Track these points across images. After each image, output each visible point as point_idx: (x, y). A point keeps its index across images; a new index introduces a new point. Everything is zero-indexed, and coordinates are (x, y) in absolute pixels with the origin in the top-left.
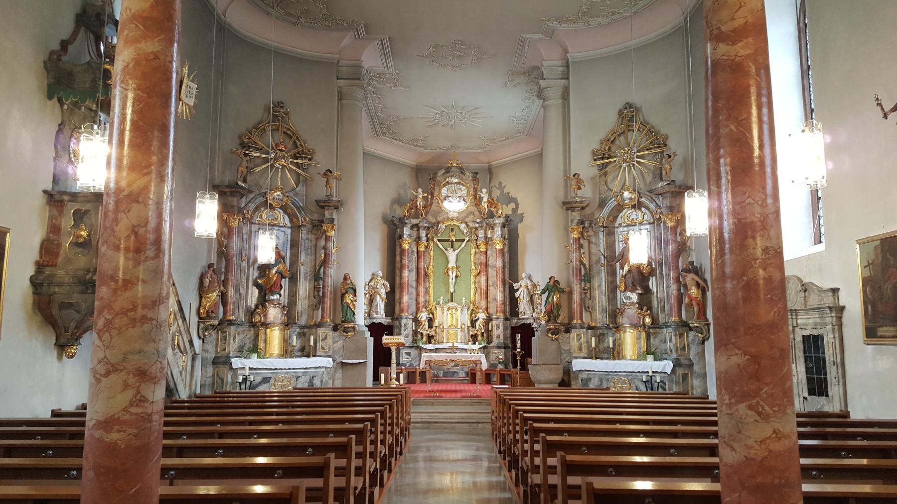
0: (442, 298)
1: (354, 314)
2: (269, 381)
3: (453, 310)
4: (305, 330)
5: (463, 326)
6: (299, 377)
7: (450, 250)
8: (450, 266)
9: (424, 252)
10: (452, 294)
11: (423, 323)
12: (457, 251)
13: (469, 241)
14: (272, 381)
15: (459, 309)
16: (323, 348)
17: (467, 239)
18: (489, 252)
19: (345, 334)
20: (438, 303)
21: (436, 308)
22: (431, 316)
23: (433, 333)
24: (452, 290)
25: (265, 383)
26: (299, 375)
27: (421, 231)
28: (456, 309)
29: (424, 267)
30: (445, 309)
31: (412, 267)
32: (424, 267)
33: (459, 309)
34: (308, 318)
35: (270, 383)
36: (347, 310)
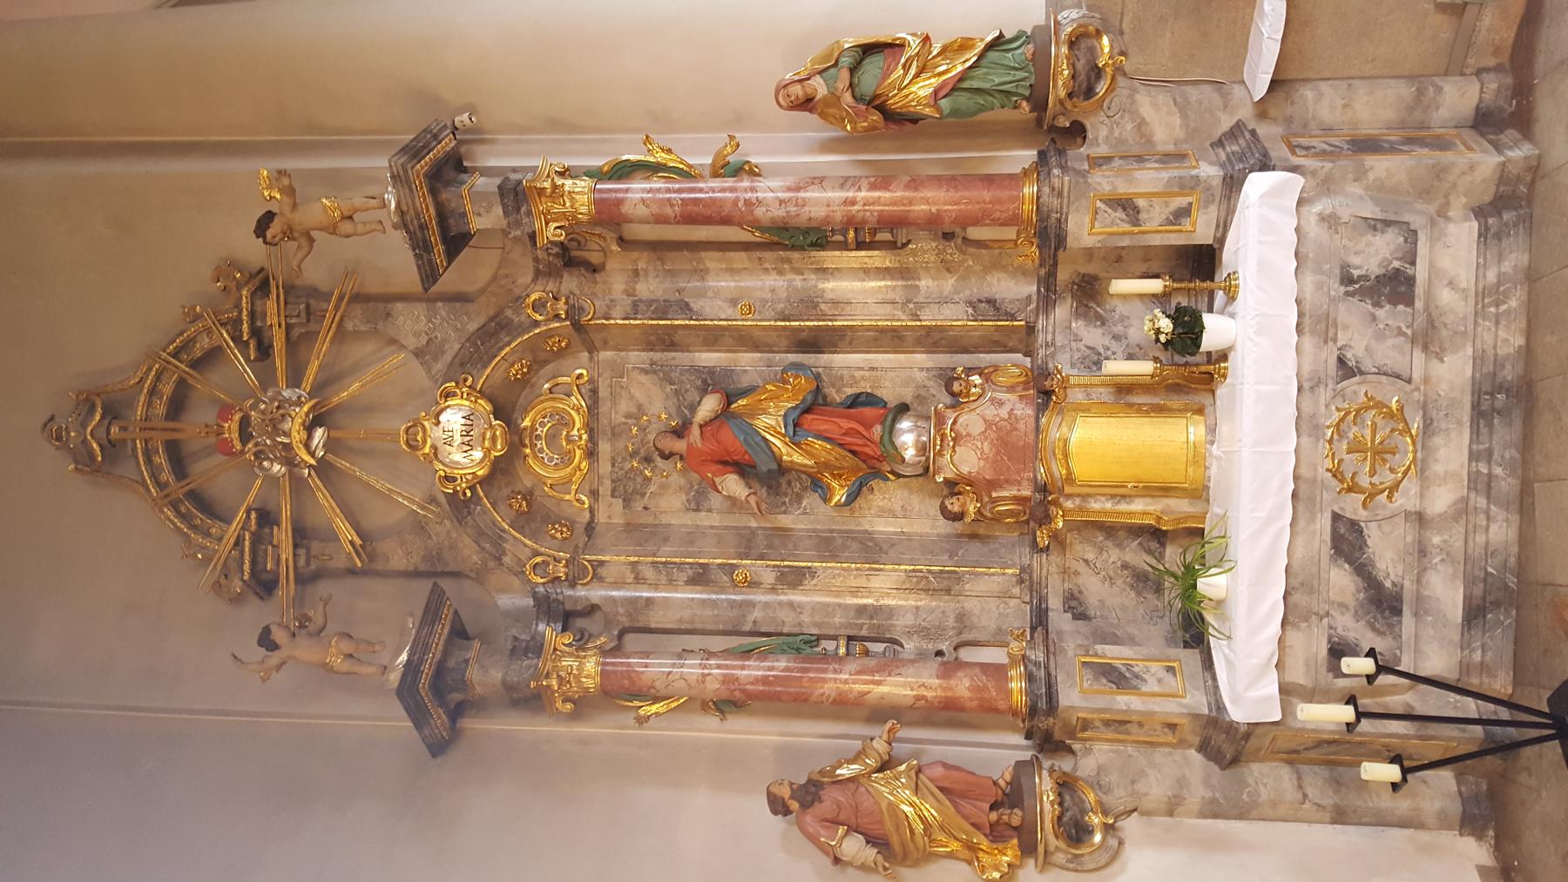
1: (998, 43)
2: (1354, 526)
4: (1063, 275)
6: (1341, 361)
14: (1352, 506)
16: (1183, 213)
19: (1101, 88)
25: (1362, 545)
26: (1333, 361)
34: (1004, 269)
35: (1362, 514)
36: (978, 91)
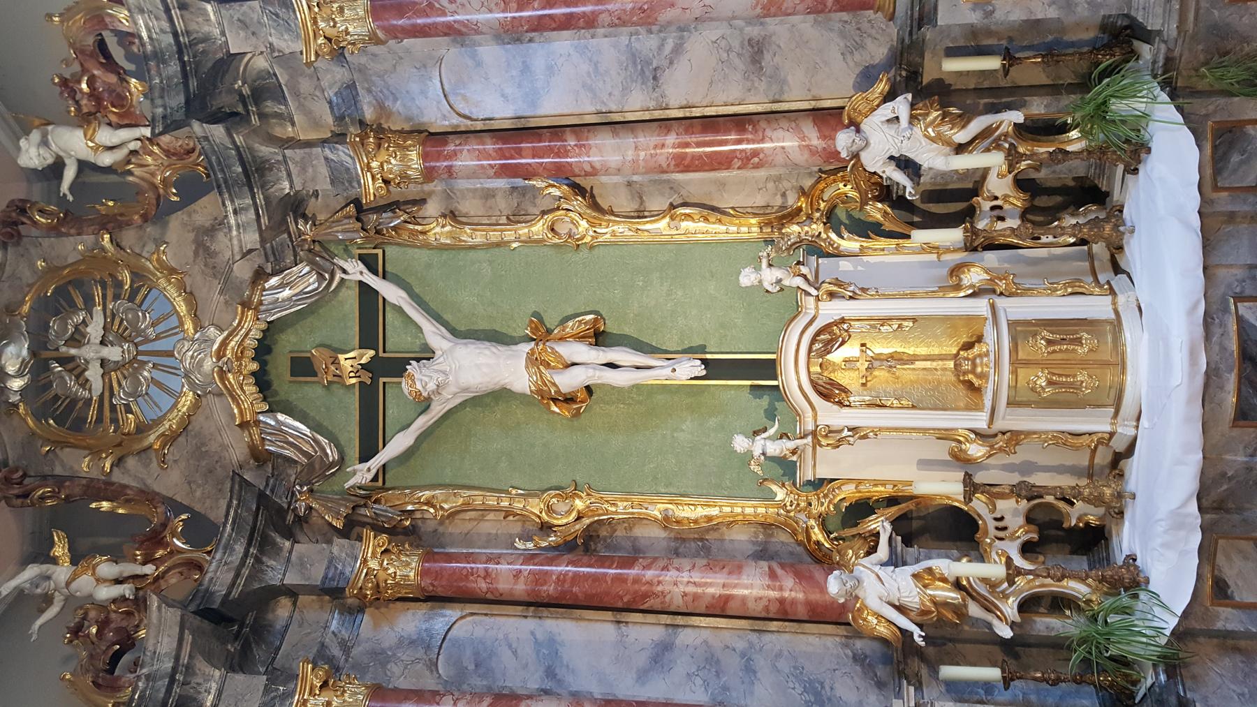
0: (740, 443)
3: (837, 356)
5: (974, 276)
7: (421, 378)
8: (519, 378)
9: (429, 556)
10: (714, 369)
11: (953, 596)
12: (434, 335)
13: (370, 263)
15: (832, 310)
17: (356, 271)
18: (437, 117)
20: (785, 467)
21: (818, 484)
22: (880, 524)
23: (1012, 510)
24: (689, 369)
27: (291, 579)
28: (829, 337)
29: (530, 558)
30: (831, 415)
31: (527, 650)
32: (530, 558)
33: (832, 310)
